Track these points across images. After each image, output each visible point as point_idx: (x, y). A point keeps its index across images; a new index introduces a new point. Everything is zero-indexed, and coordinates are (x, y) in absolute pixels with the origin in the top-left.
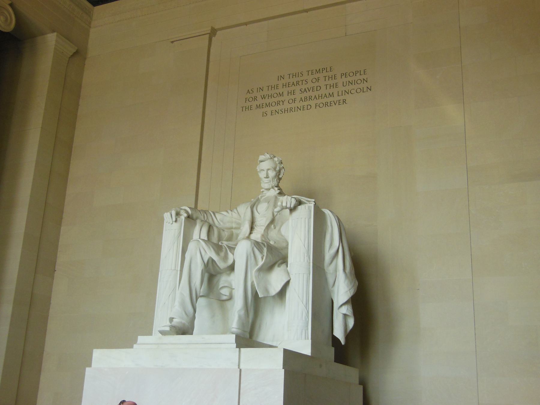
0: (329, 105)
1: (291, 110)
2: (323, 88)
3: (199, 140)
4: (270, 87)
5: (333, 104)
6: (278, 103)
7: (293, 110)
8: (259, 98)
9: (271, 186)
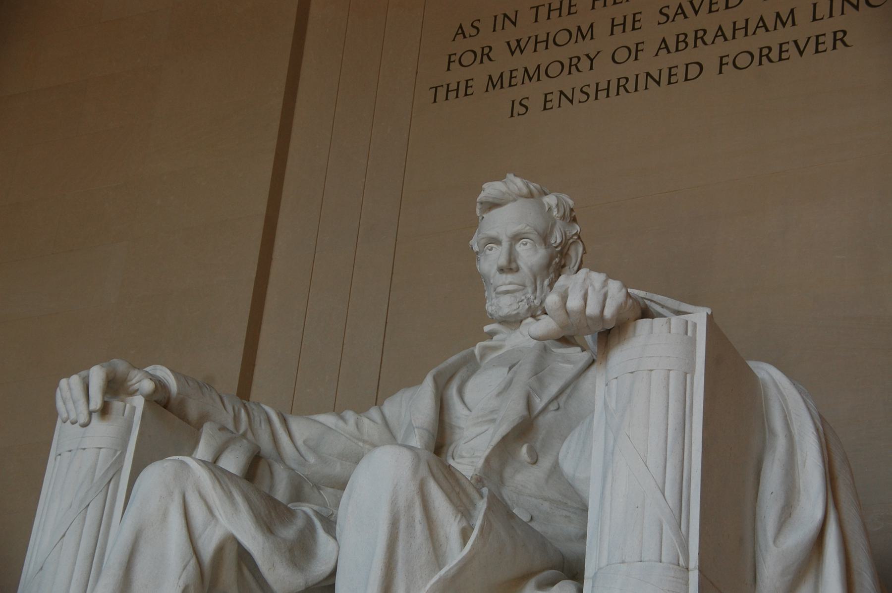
0: (774, 55)
3: (262, 208)
4: (543, 11)
6: (573, 65)
7: (631, 86)
8: (500, 52)
9: (524, 306)
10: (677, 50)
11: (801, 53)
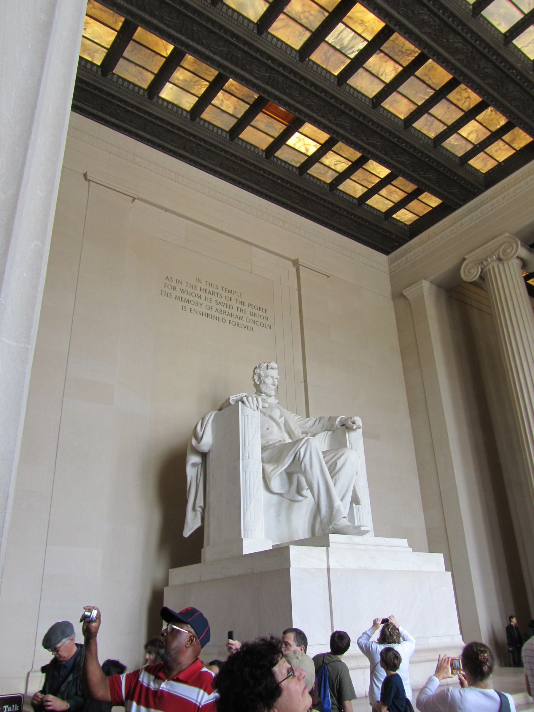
0: (240, 325)
5: (243, 327)
6: (196, 303)
7: (210, 316)
8: (178, 289)
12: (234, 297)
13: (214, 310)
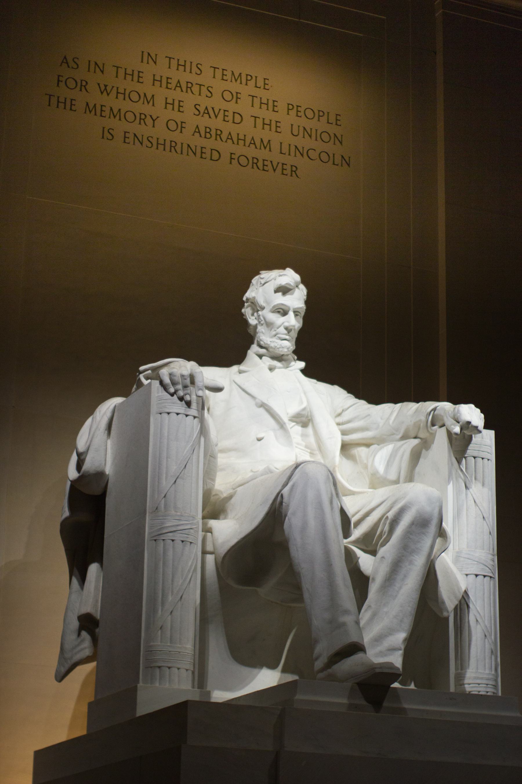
0: (260, 164)
1: (173, 145)
2: (248, 122)
4: (121, 72)
5: (270, 167)
6: (142, 118)
7: (178, 148)
10: (205, 137)
11: (275, 170)
12: (246, 91)
13: (189, 129)
